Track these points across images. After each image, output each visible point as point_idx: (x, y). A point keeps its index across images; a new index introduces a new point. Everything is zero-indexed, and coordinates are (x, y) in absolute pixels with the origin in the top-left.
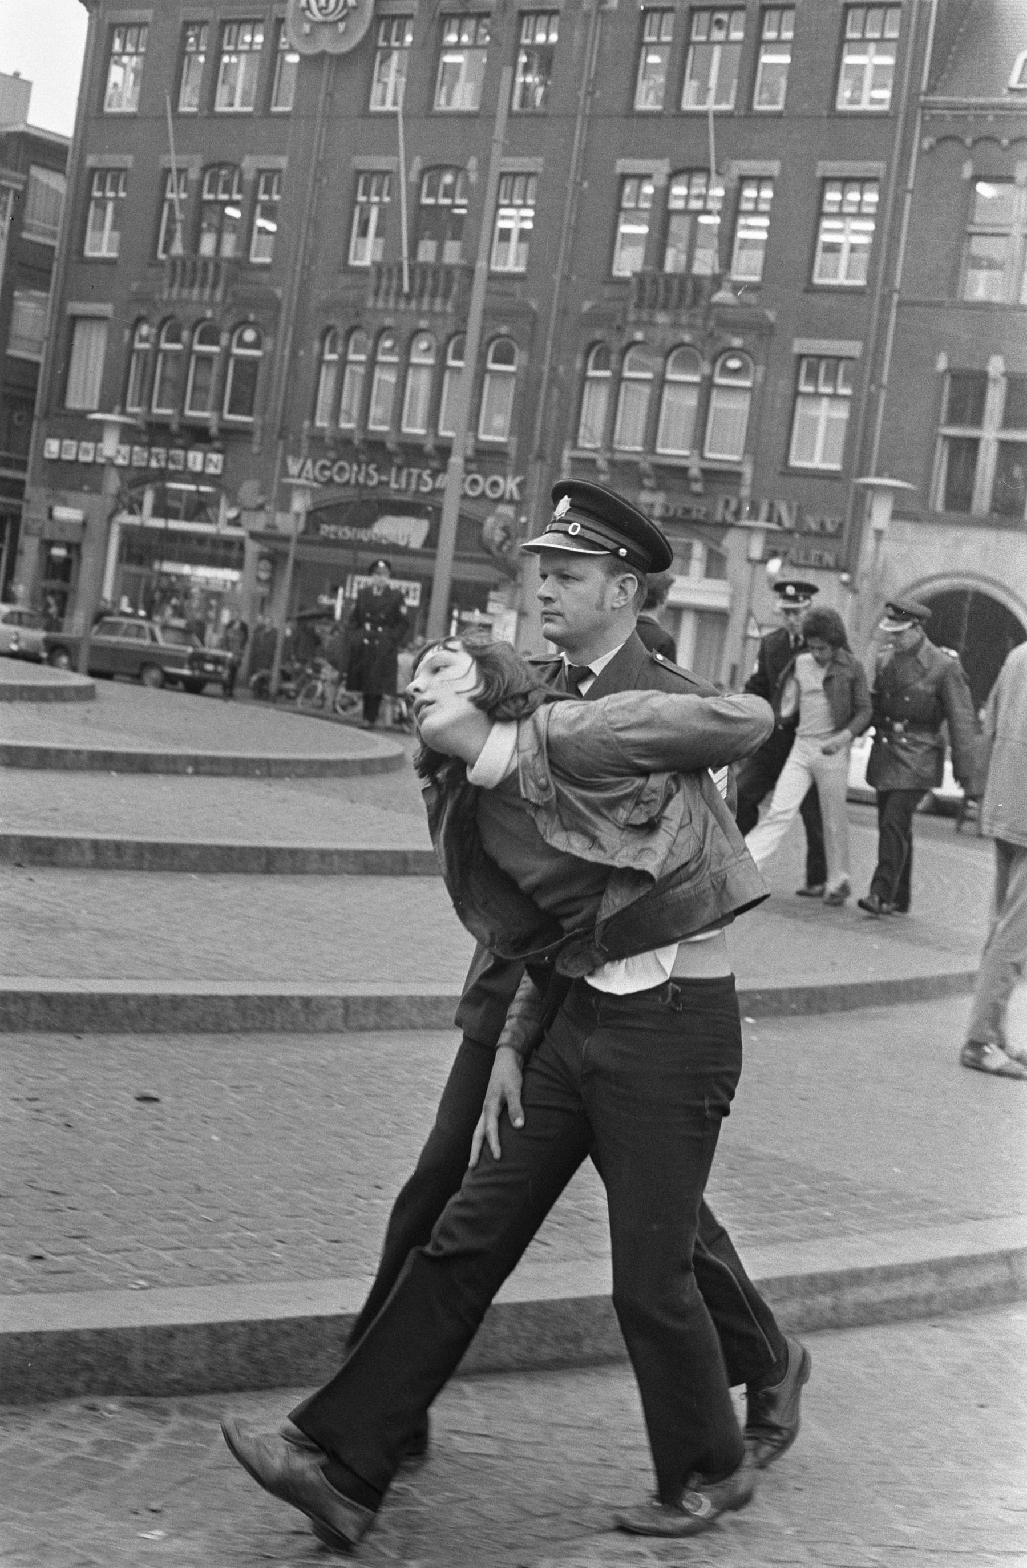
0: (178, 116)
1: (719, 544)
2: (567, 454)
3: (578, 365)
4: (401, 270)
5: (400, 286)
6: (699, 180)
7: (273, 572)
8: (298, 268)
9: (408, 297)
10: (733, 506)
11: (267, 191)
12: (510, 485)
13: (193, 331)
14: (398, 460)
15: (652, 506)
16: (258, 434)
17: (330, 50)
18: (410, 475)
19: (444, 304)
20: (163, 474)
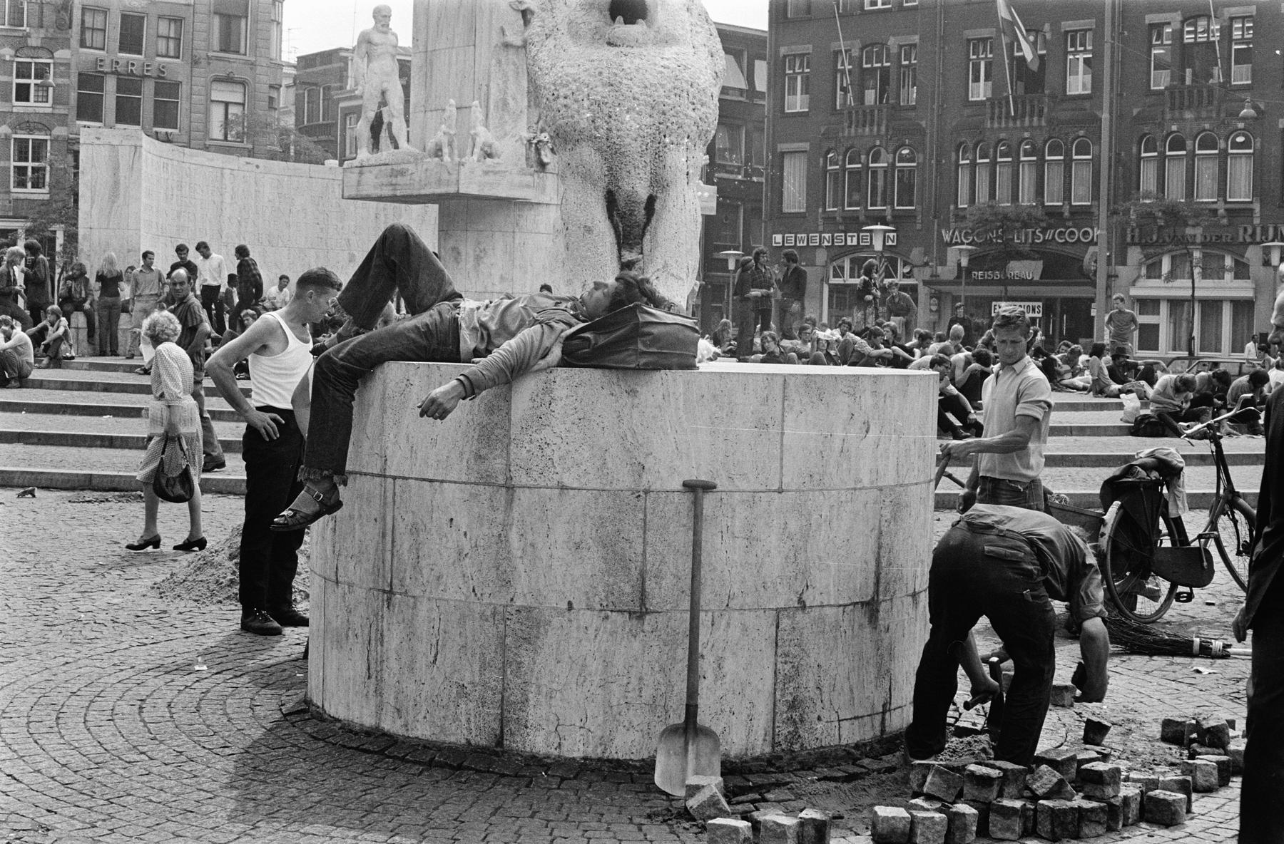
3: (1134, 150)
4: (1008, 102)
5: (1008, 112)
7: (939, 305)
8: (935, 106)
10: (1250, 231)
11: (908, 58)
13: (868, 155)
16: (919, 217)
18: (1026, 235)
19: (1039, 121)
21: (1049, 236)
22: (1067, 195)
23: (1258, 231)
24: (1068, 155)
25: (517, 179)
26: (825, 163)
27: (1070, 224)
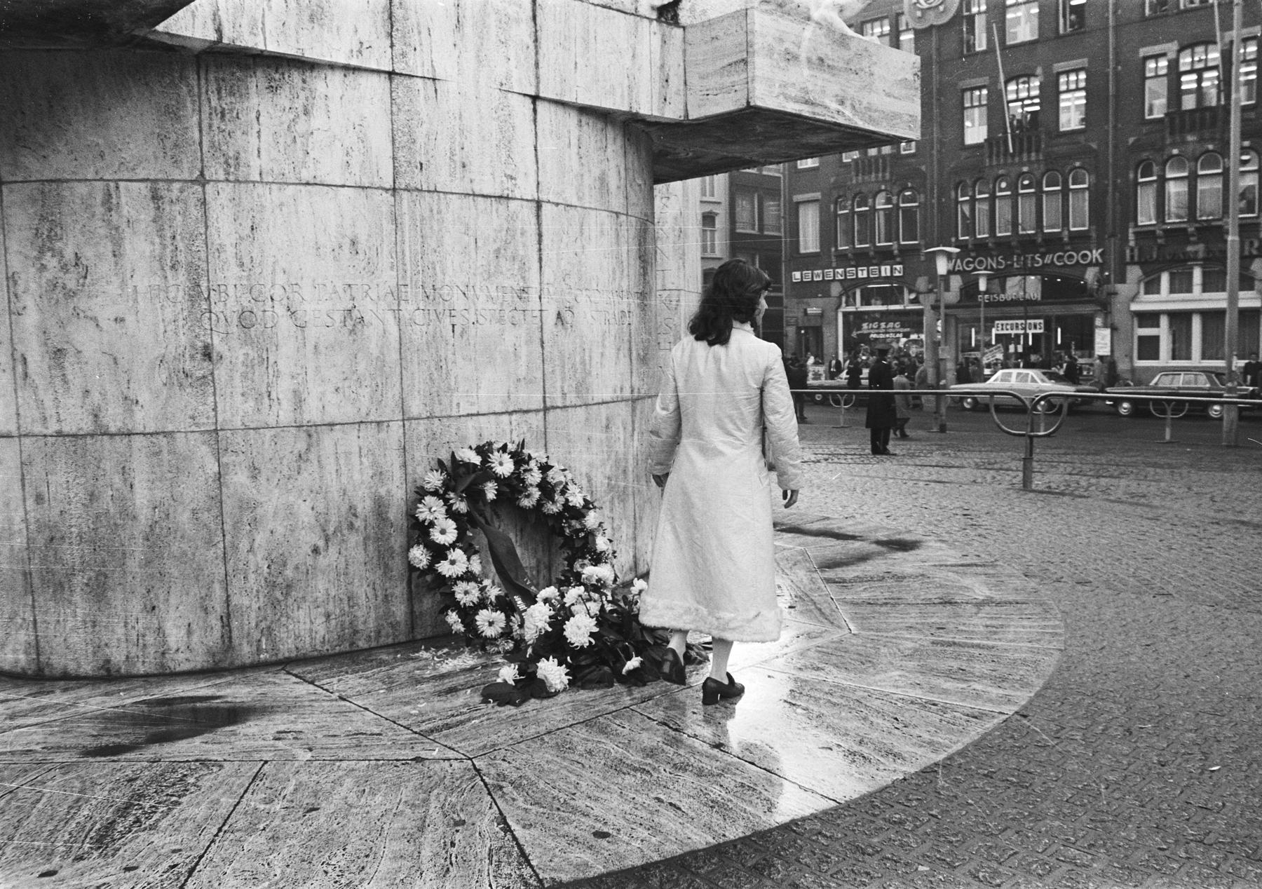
2: (1131, 230)
3: (1131, 176)
6: (1200, 49)
8: (935, 152)
9: (1013, 156)
12: (1096, 254)
14: (1042, 250)
15: (1196, 252)
20: (868, 280)
21: (1048, 260)
22: (1065, 223)
24: (1065, 184)
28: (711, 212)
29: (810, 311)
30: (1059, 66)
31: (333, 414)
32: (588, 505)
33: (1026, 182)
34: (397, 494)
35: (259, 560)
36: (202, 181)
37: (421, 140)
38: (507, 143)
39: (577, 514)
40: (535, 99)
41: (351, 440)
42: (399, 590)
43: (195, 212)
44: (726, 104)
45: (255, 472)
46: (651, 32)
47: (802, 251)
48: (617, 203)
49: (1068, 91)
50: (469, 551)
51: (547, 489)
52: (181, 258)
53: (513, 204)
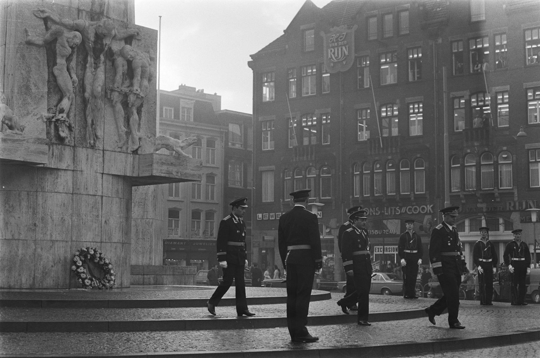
0: (290, 100)
1: (509, 218)
6: (481, 95)
8: (340, 144)
10: (512, 205)
12: (429, 208)
13: (306, 171)
17: (341, 71)
18: (391, 209)
21: (403, 210)
22: (412, 189)
23: (517, 204)
25: (33, 147)
26: (283, 176)
27: (415, 204)
28: (212, 173)
29: (266, 238)
30: (408, 100)
31: (58, 238)
32: (110, 263)
33: (390, 165)
34: (69, 256)
35: (41, 267)
36: (37, 191)
37: (78, 183)
38: (96, 184)
39: (107, 265)
40: (103, 174)
41: (61, 244)
42: (68, 277)
43: (35, 197)
44: (147, 174)
45: (42, 249)
46: (130, 158)
47: (264, 201)
48: (121, 195)
49: (414, 113)
50: (84, 268)
51: (100, 258)
52: (32, 206)
53: (97, 197)
